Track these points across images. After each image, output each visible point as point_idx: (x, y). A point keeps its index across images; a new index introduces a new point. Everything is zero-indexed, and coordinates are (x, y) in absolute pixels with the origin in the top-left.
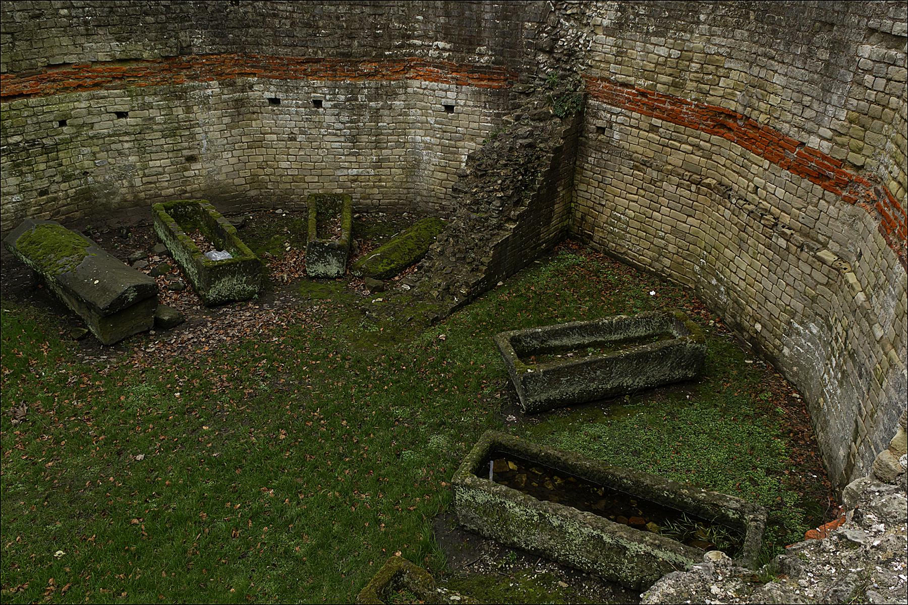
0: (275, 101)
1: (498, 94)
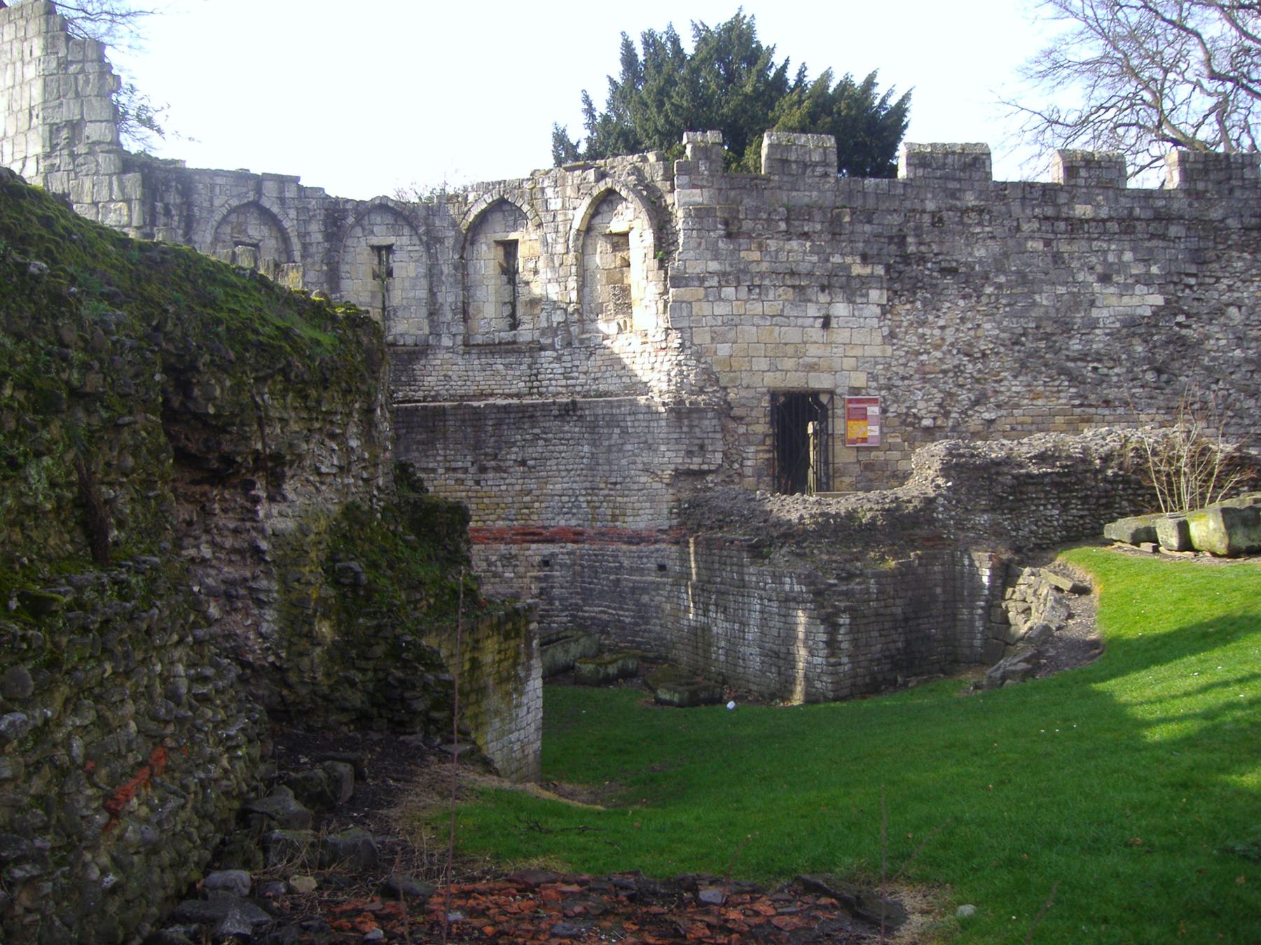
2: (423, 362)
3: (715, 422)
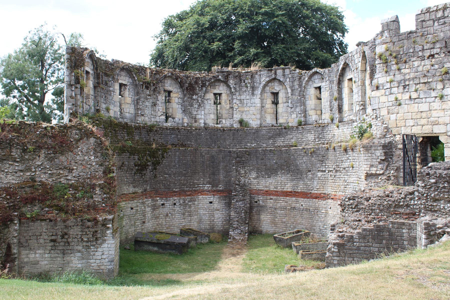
0: (163, 204)
1: (225, 197)
2: (327, 129)
3: (381, 151)
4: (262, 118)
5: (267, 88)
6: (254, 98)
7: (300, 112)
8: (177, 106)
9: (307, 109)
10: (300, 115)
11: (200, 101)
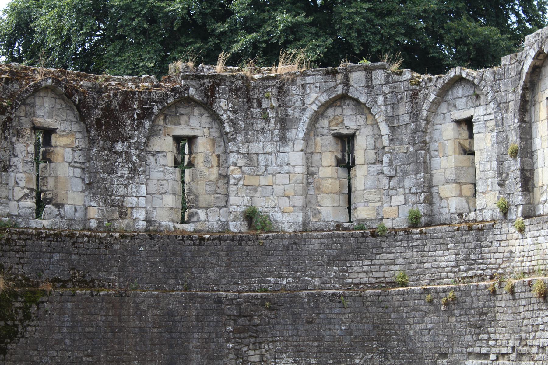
2: (490, 238)
4: (309, 206)
5: (324, 123)
6: (287, 149)
7: (413, 190)
8: (71, 172)
9: (435, 181)
10: (414, 199)
11: (134, 158)
